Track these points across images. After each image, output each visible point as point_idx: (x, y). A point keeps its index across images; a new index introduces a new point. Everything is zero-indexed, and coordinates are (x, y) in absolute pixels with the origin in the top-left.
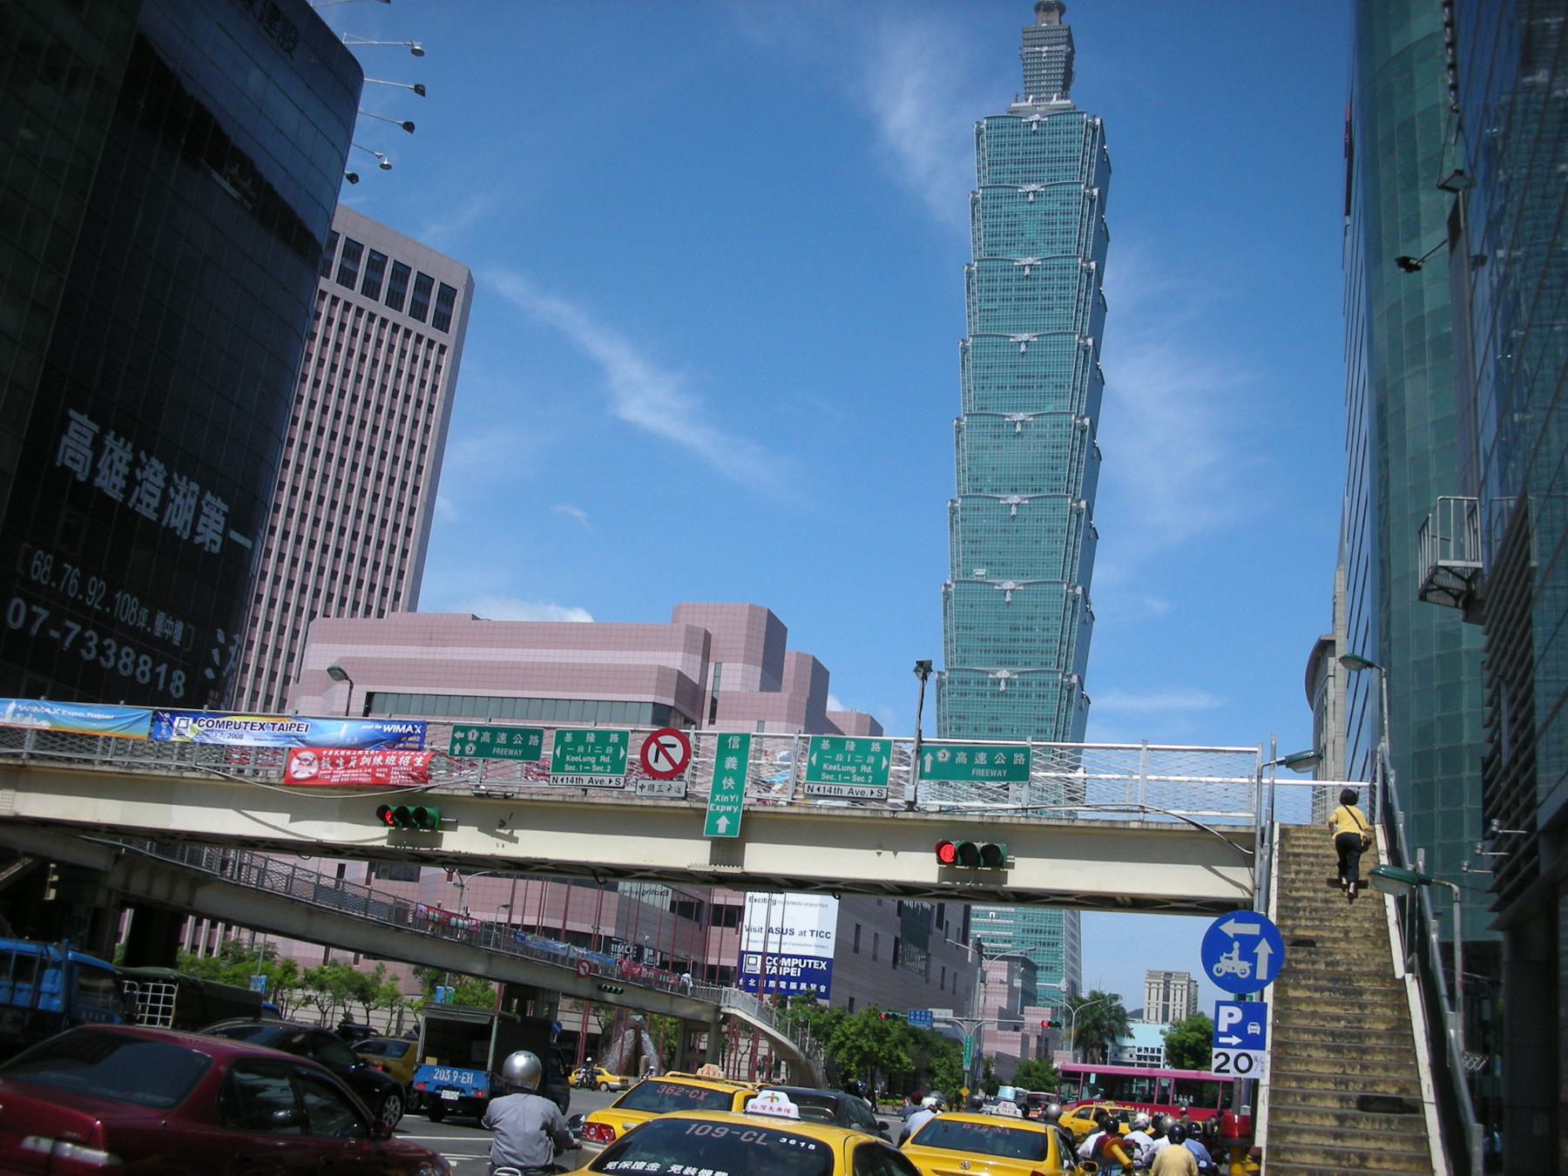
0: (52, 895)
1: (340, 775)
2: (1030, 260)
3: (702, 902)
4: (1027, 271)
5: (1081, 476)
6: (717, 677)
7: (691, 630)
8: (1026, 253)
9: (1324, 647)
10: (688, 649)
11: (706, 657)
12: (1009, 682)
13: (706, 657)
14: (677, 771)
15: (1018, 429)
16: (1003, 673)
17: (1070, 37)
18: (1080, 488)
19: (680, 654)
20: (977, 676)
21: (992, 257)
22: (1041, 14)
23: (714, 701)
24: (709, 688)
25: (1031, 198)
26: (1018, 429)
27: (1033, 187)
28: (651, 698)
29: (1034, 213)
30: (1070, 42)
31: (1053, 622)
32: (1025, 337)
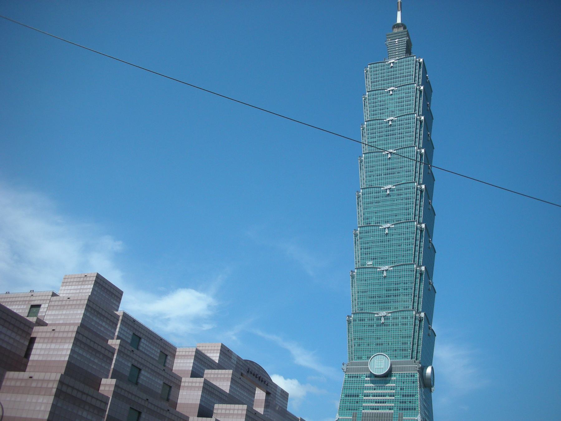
5: (422, 213)
15: (388, 192)
16: (383, 313)
18: (421, 219)
20: (368, 316)
26: (388, 192)
27: (393, 88)
30: (408, 35)
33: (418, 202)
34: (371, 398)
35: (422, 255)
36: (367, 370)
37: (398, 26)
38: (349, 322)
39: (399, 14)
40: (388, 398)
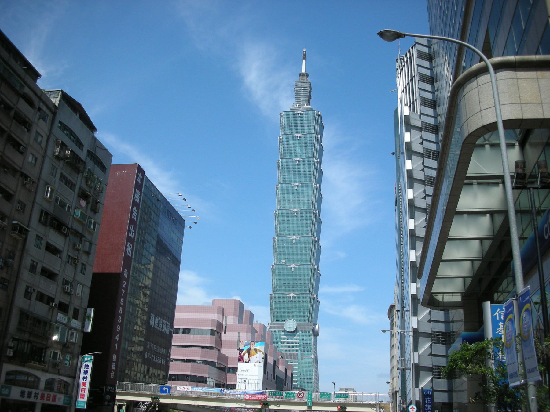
0: (157, 409)
1: (253, 398)
2: (298, 159)
3: (224, 384)
4: (297, 162)
6: (226, 320)
7: (219, 308)
8: (297, 156)
9: (392, 307)
10: (218, 313)
11: (223, 315)
12: (294, 297)
13: (223, 315)
14: (302, 397)
15: (295, 214)
16: (292, 294)
17: (310, 85)
18: (315, 233)
19: (216, 315)
20: (282, 295)
21: (286, 158)
22: (301, 77)
23: (226, 327)
24: (224, 323)
25: (298, 138)
26: (295, 214)
27: (299, 135)
28: (210, 328)
29: (299, 143)
30: (310, 87)
31: (308, 277)
32: (297, 184)
33: (314, 222)
34: (285, 344)
35: (315, 258)
36: (283, 328)
37: (302, 75)
38: (271, 298)
39: (304, 61)
40: (295, 344)
